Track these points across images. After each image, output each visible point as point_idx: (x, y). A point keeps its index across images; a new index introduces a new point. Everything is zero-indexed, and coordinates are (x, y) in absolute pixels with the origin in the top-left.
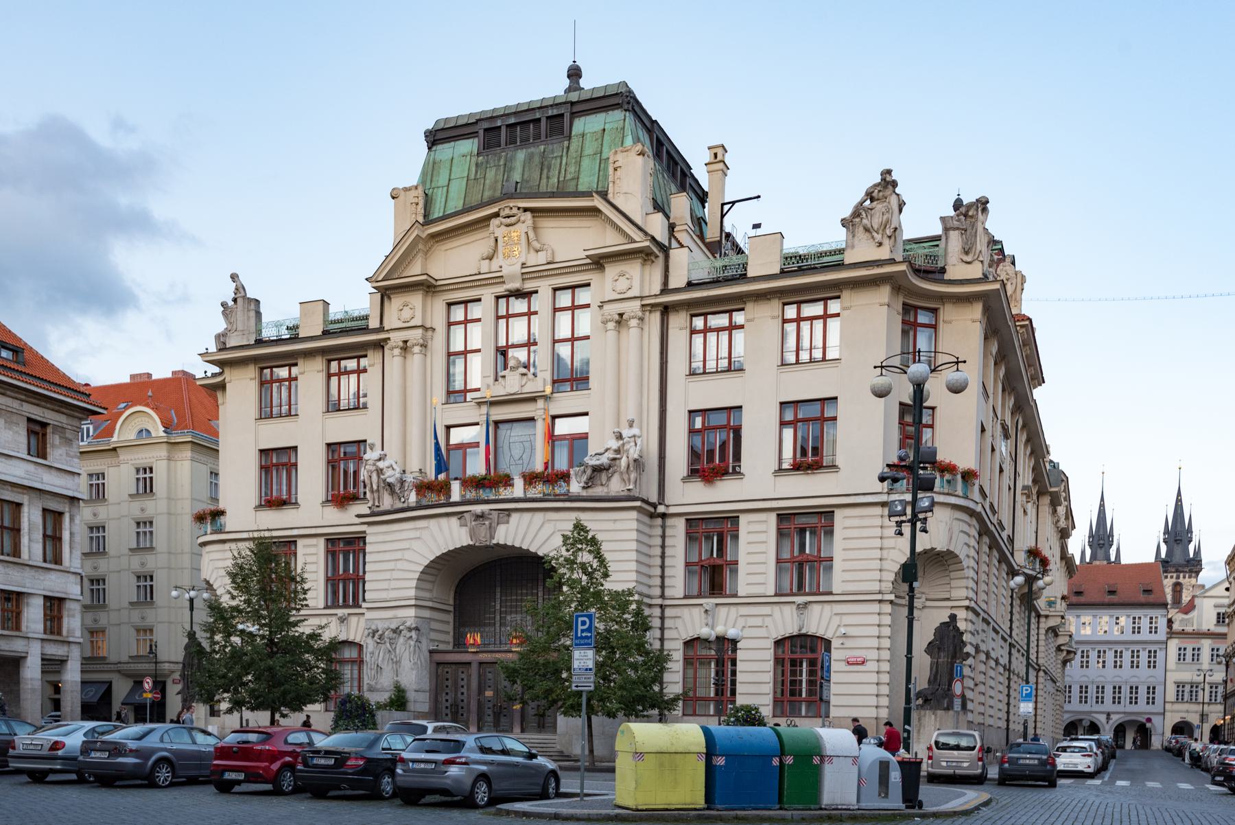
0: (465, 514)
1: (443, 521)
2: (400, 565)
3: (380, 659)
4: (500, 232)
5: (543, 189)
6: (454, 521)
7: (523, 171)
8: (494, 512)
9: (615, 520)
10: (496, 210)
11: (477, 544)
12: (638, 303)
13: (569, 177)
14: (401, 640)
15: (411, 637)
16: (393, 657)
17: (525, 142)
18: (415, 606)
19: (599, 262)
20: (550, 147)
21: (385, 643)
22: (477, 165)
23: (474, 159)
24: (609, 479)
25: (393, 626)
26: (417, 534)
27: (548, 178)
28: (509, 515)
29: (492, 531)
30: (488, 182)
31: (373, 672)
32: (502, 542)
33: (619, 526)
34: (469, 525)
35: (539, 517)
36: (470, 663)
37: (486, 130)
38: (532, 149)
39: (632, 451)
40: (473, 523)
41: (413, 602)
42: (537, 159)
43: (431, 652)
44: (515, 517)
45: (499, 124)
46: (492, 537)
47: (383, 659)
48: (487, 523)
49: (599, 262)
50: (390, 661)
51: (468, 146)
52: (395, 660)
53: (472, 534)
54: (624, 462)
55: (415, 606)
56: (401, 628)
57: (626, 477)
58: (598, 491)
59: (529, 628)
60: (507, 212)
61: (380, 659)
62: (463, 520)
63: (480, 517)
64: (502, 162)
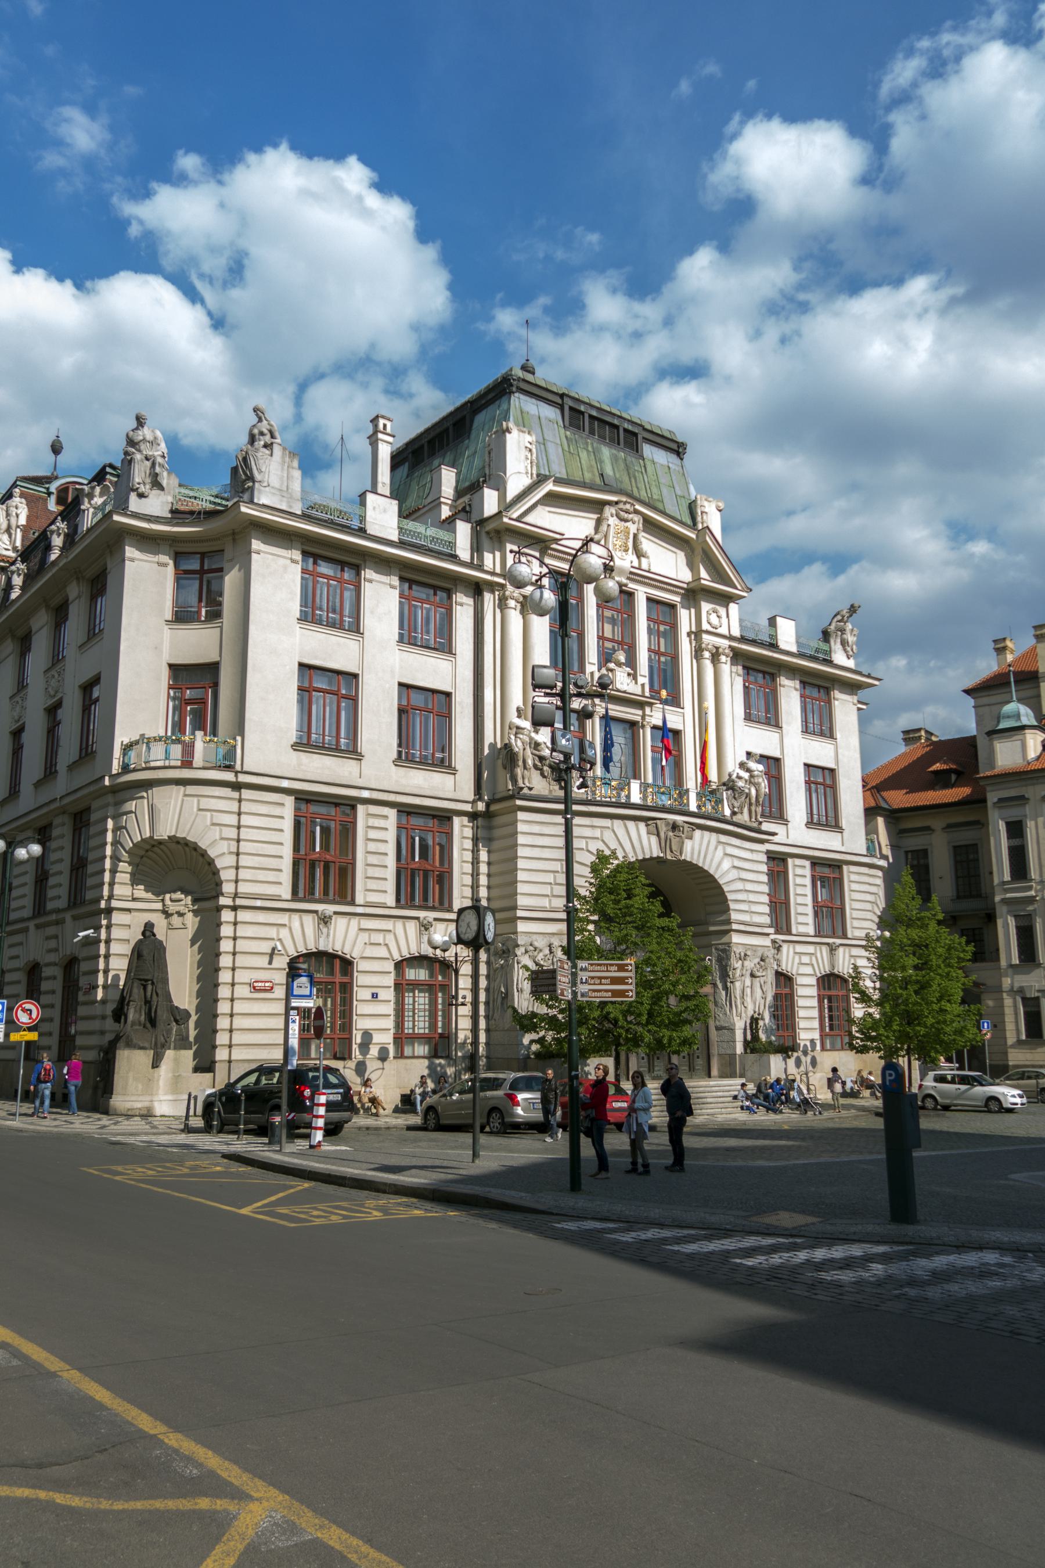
0: (658, 821)
1: (631, 824)
4: (613, 521)
5: (636, 493)
6: (642, 825)
7: (613, 469)
8: (686, 825)
9: (752, 851)
10: (614, 498)
11: (669, 857)
12: (724, 643)
13: (655, 497)
17: (602, 437)
19: (693, 594)
20: (629, 458)
22: (566, 437)
23: (562, 431)
26: (597, 833)
27: (638, 488)
28: (694, 830)
29: (683, 843)
30: (583, 462)
32: (688, 859)
34: (662, 835)
37: (571, 408)
38: (614, 451)
39: (763, 785)
42: (622, 466)
45: (582, 408)
46: (681, 854)
49: (693, 594)
51: (550, 413)
53: (665, 844)
54: (753, 792)
58: (736, 819)
60: (628, 506)
62: (653, 829)
64: (590, 449)
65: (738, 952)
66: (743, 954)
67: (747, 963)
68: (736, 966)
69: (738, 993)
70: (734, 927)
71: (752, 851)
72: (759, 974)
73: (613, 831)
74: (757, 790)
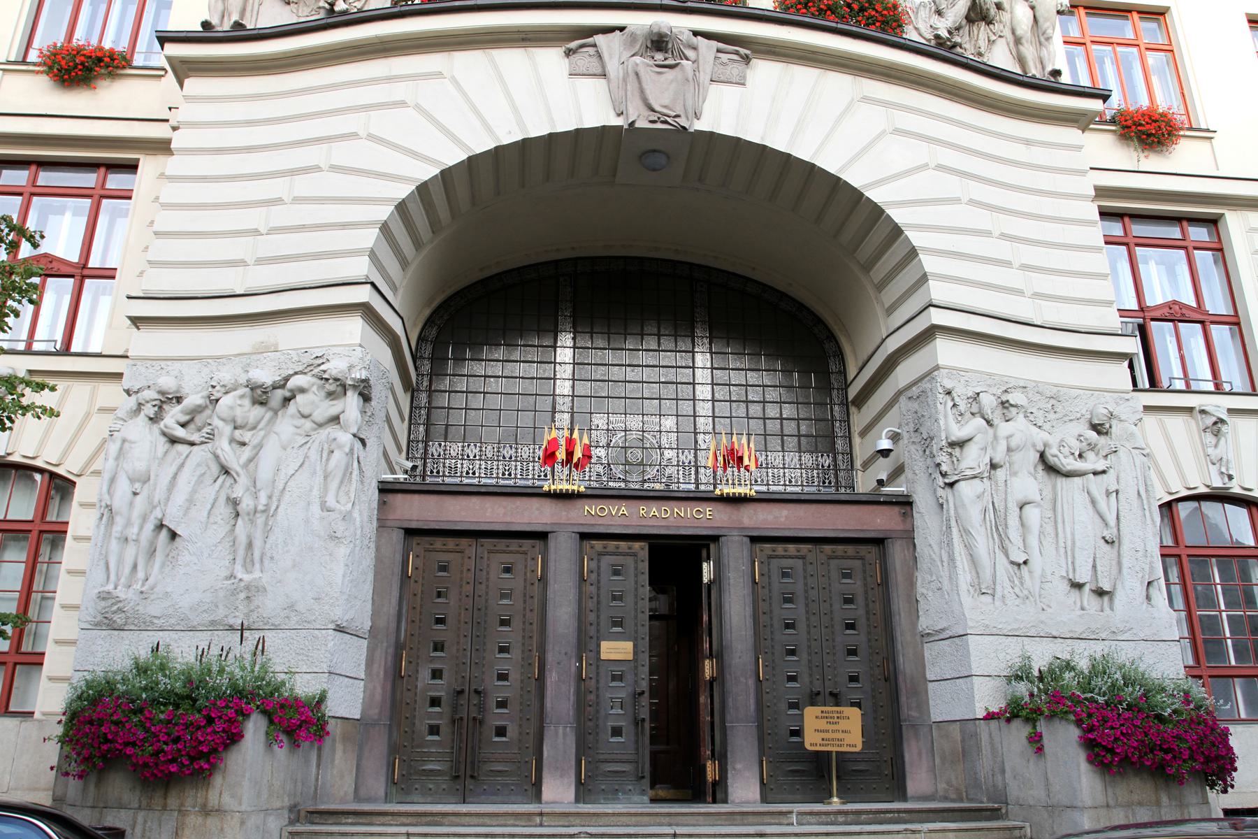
0: (599, 39)
1: (510, 59)
2: (303, 186)
3: (180, 497)
6: (551, 59)
9: (1028, 142)
11: (642, 124)
14: (286, 425)
15: (335, 419)
16: (238, 492)
18: (366, 310)
21: (211, 436)
24: (991, 42)
25: (265, 375)
26: (399, 91)
28: (747, 60)
31: (130, 552)
32: (726, 129)
33: (1038, 155)
34: (613, 67)
35: (840, 84)
36: (542, 536)
40: (638, 59)
41: (363, 294)
43: (386, 489)
44: (764, 71)
46: (697, 116)
47: (191, 501)
48: (684, 62)
50: (224, 511)
52: (246, 504)
55: (366, 310)
56: (294, 382)
57: (1029, 51)
59: (669, 454)
61: (180, 497)
62: (584, 60)
63: (659, 43)
65: (962, 391)
66: (988, 401)
67: (1004, 428)
68: (958, 433)
69: (974, 515)
70: (938, 317)
71: (1028, 142)
72: (1070, 464)
73: (454, 81)
74: (1033, 8)
